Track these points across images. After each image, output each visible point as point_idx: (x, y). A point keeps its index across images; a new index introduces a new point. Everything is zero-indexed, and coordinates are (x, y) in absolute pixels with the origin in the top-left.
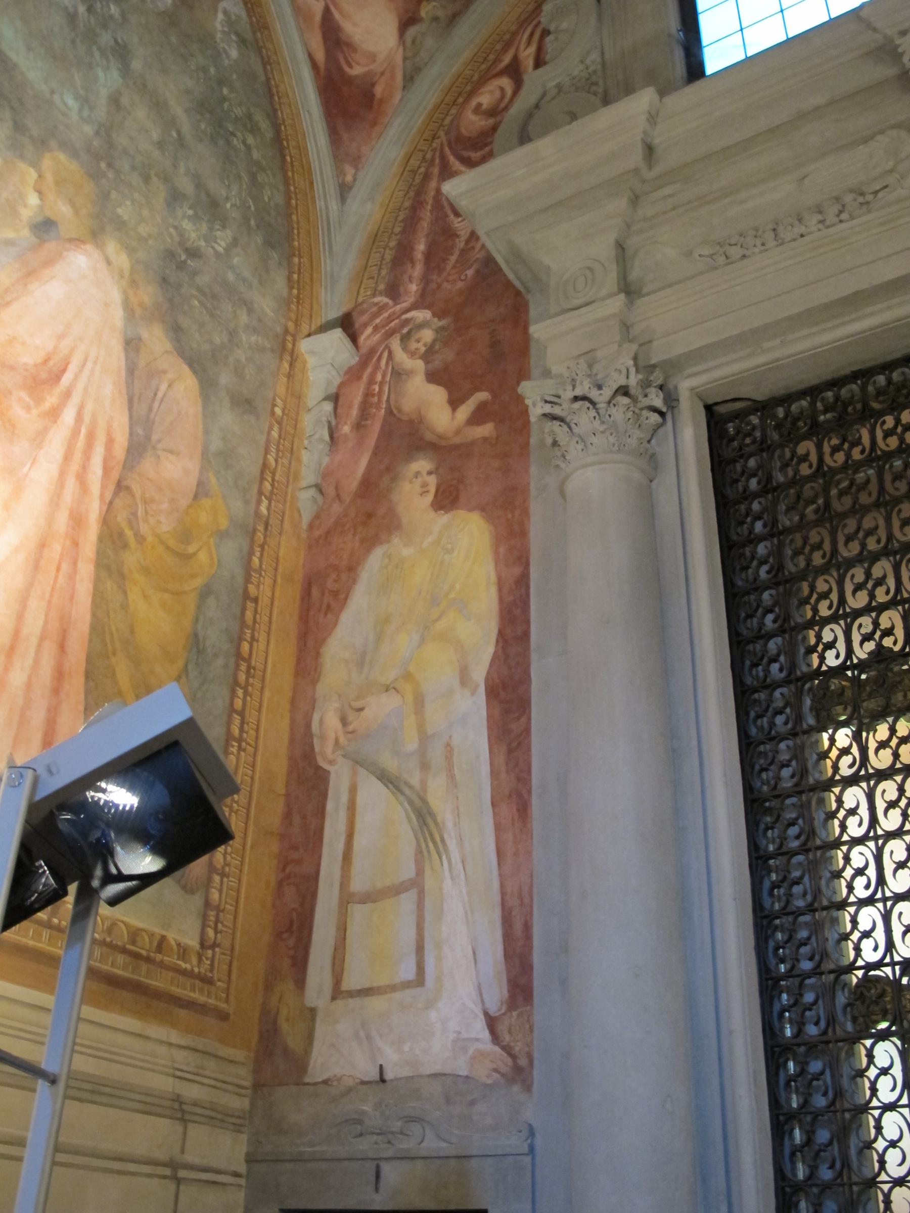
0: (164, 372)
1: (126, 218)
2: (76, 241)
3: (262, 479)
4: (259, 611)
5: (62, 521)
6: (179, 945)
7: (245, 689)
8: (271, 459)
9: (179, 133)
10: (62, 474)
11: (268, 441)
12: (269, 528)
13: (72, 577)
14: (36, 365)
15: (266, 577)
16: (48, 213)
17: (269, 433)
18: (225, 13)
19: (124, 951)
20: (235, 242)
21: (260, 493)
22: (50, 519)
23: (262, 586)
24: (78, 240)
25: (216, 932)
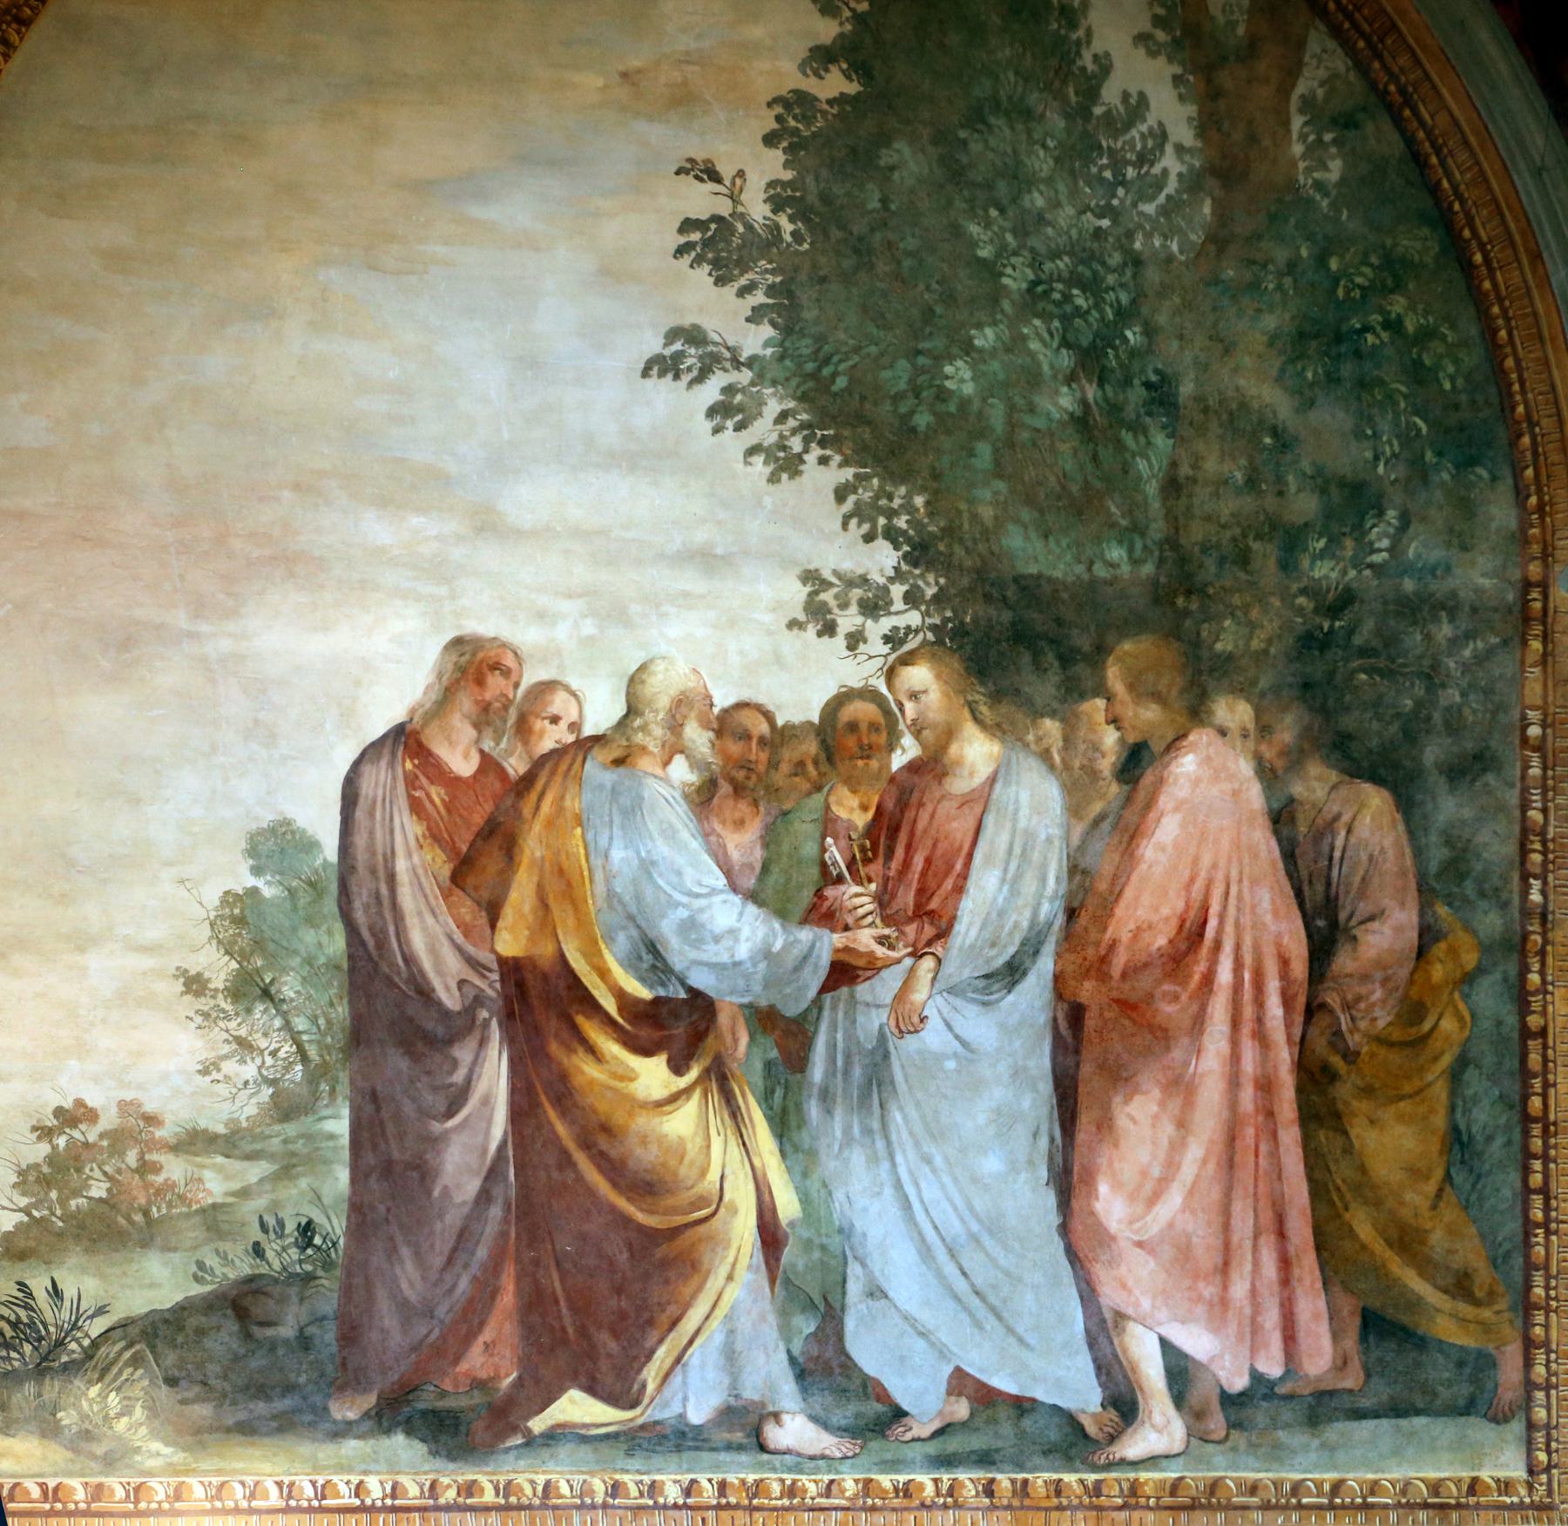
0: (1337, 818)
1: (1230, 648)
2: (1174, 744)
3: (1524, 852)
4: (1551, 1043)
5: (1247, 1096)
6: (1498, 1481)
7: (1546, 1159)
8: (1535, 815)
9: (1275, 432)
10: (1235, 1043)
11: (1525, 791)
12: (1550, 917)
13: (1275, 1154)
14: (1171, 942)
15: (1556, 992)
16: (1131, 739)
17: (1523, 777)
18: (1308, 104)
19: (1426, 1506)
20: (1405, 520)
21: (1525, 877)
22: (1233, 1104)
23: (1550, 1008)
24: (1177, 739)
25: (1549, 1452)
